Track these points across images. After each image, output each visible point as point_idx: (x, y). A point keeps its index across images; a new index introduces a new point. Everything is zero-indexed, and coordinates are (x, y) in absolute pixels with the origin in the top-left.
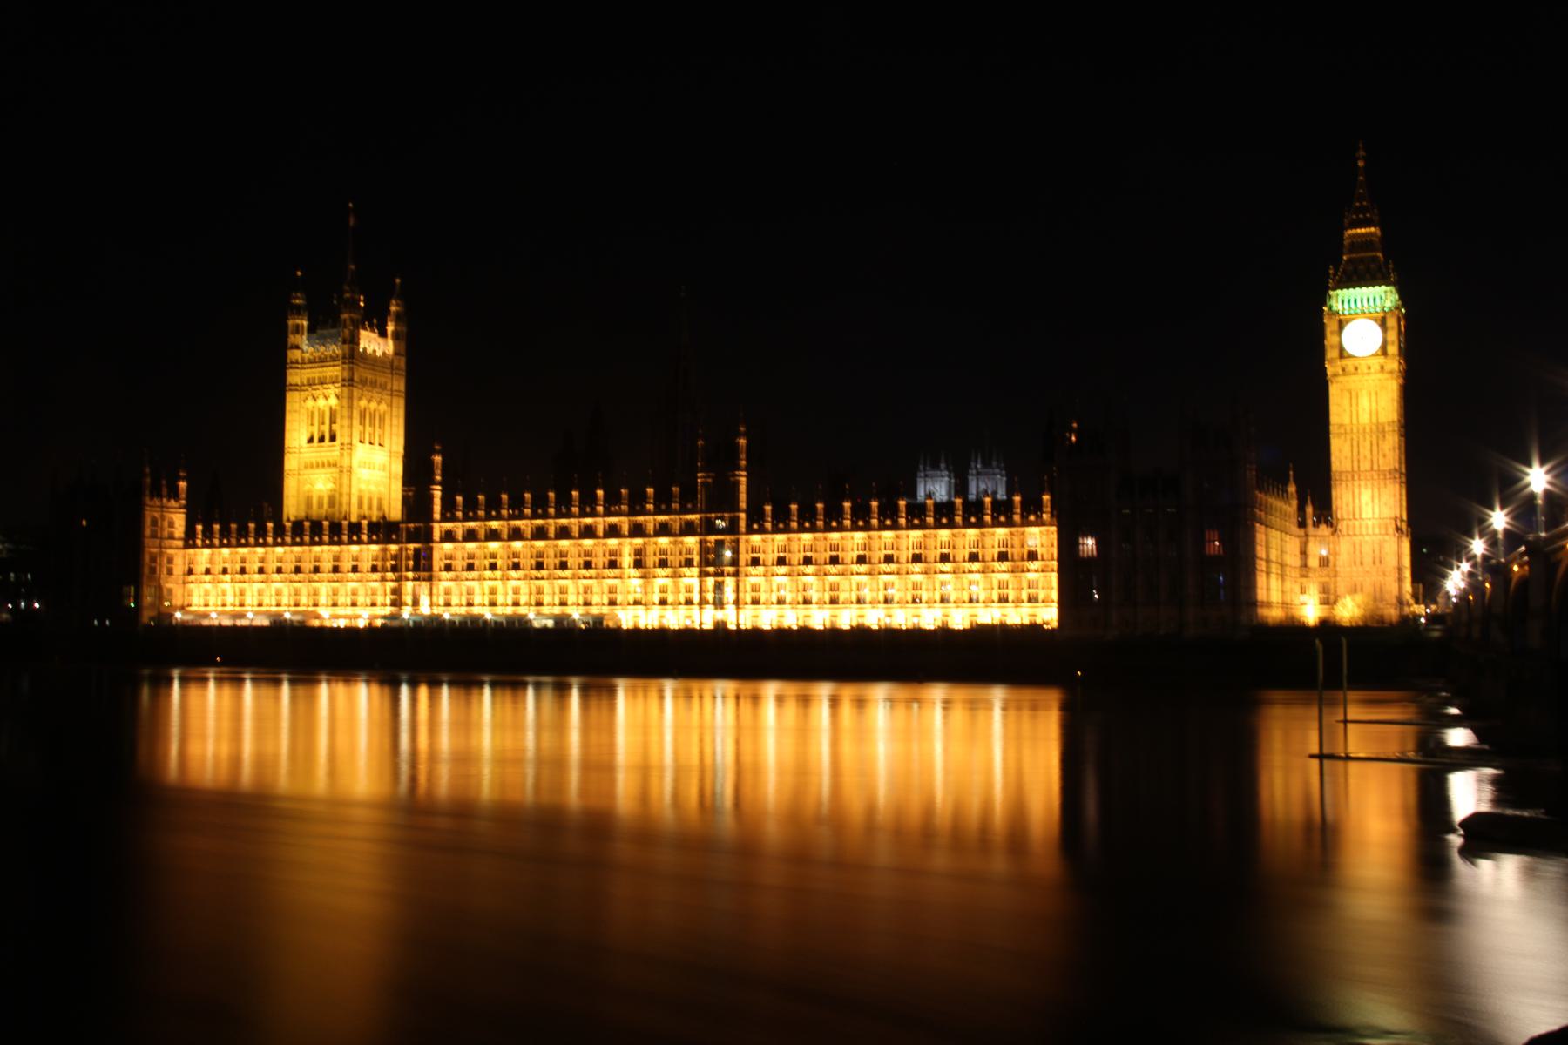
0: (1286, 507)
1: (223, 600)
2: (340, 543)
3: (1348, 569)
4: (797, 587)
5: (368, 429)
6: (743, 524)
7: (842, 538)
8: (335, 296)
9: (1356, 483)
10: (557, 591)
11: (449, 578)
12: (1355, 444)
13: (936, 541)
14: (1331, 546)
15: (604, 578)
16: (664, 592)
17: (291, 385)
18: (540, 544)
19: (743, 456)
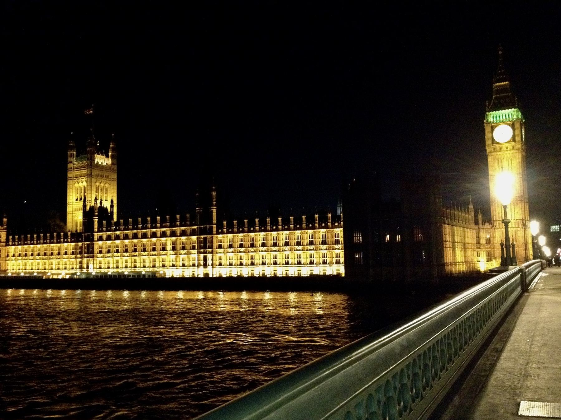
1: (32, 267)
2: (60, 242)
4: (237, 257)
6: (215, 230)
14: (491, 233)
15: (160, 255)
16: (184, 261)
17: (69, 178)
18: (135, 241)
19: (214, 200)
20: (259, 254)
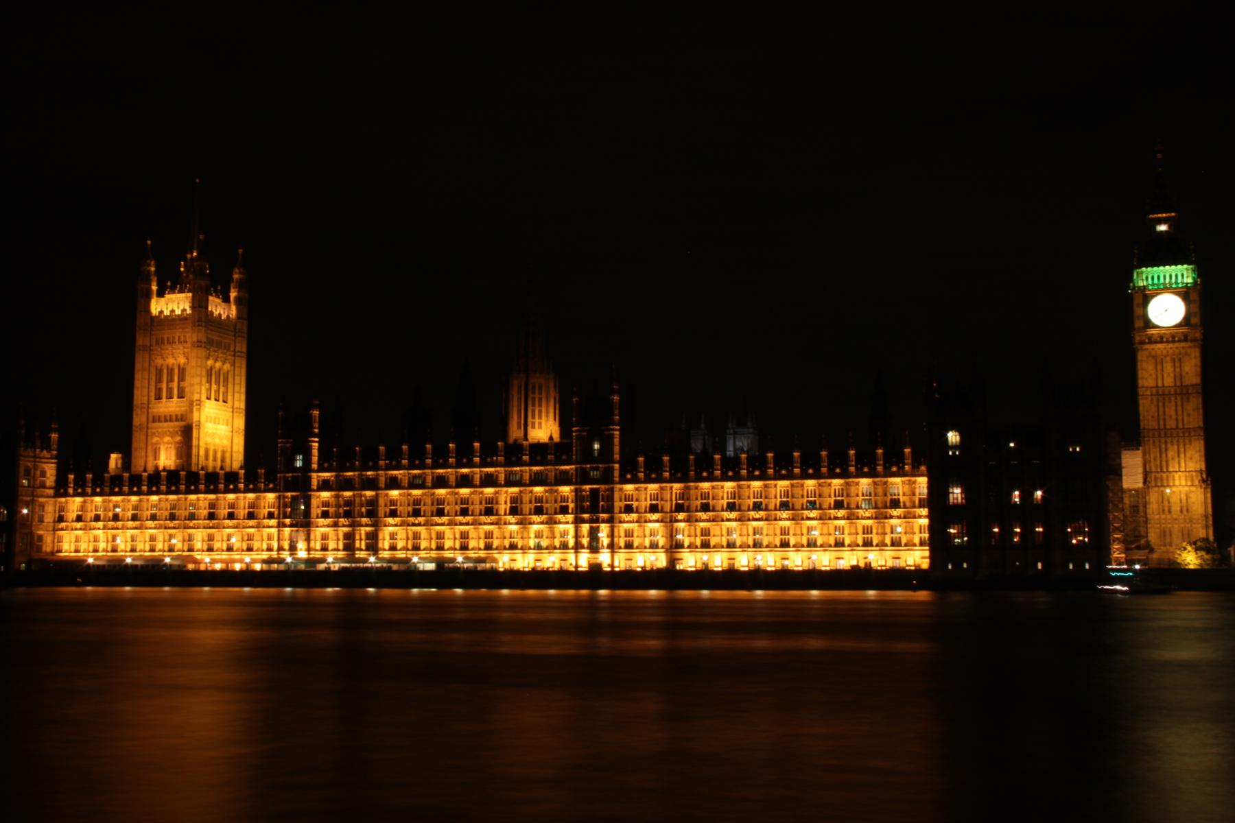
2: (215, 491)
3: (1157, 517)
5: (214, 387)
6: (617, 473)
8: (182, 263)
10: (434, 536)
11: (325, 524)
12: (1161, 404)
13: (803, 490)
15: (480, 524)
19: (617, 412)
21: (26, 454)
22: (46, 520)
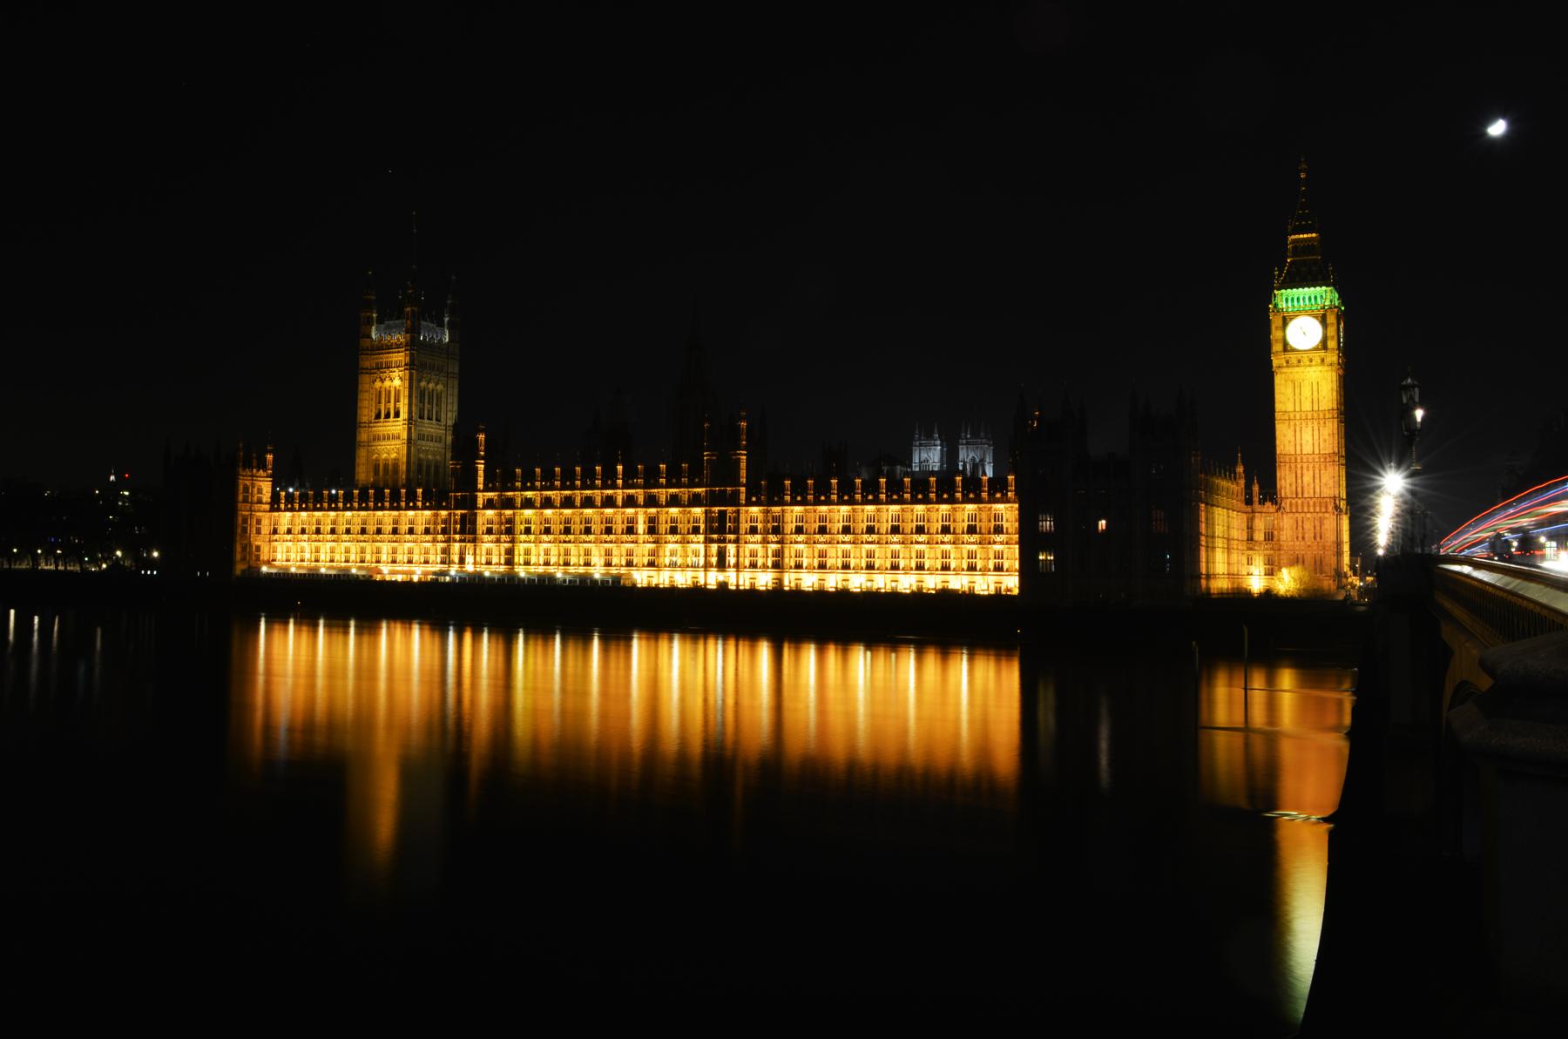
0: (1232, 488)
2: (398, 508)
6: (743, 496)
7: (830, 511)
9: (1299, 466)
10: (582, 553)
12: (1298, 429)
15: (622, 543)
18: (567, 512)
20: (837, 548)
21: (244, 474)
22: (263, 533)
